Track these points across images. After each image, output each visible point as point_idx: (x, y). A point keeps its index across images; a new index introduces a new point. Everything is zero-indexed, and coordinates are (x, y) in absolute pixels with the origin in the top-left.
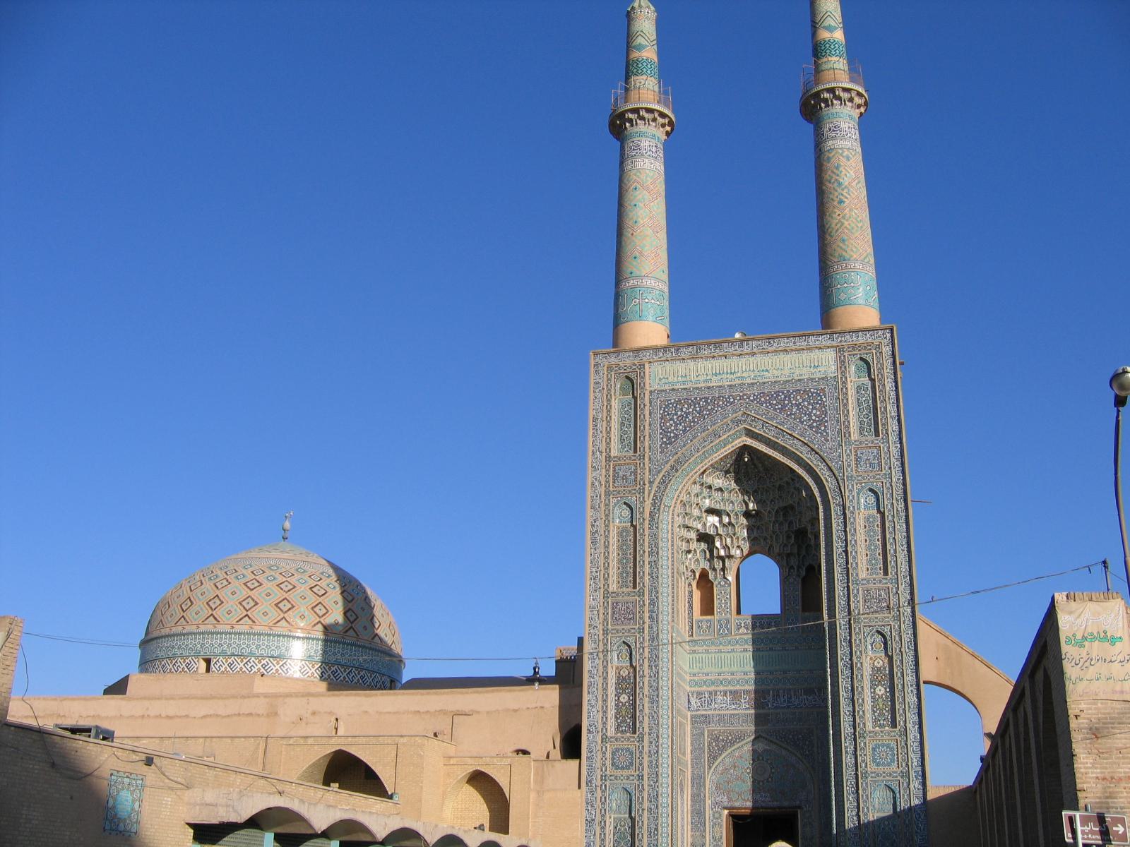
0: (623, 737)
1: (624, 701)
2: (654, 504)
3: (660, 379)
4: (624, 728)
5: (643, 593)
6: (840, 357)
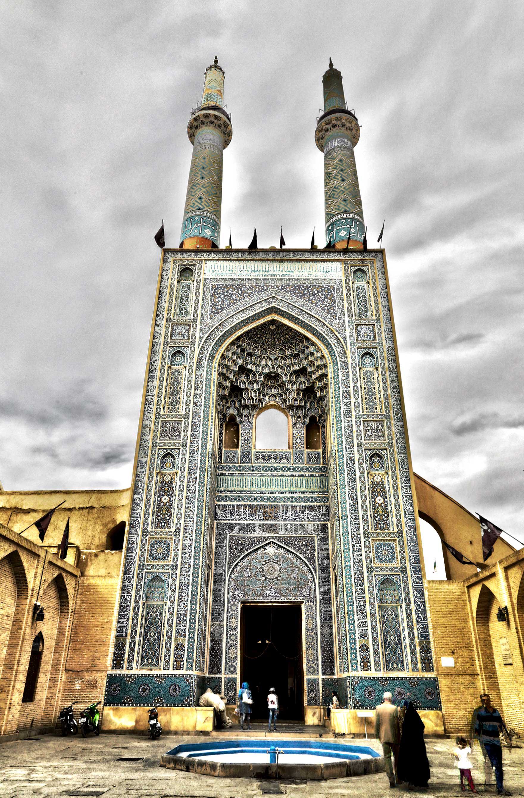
0: (161, 532)
1: (165, 501)
2: (201, 353)
3: (213, 271)
4: (163, 524)
5: (189, 416)
6: (345, 267)
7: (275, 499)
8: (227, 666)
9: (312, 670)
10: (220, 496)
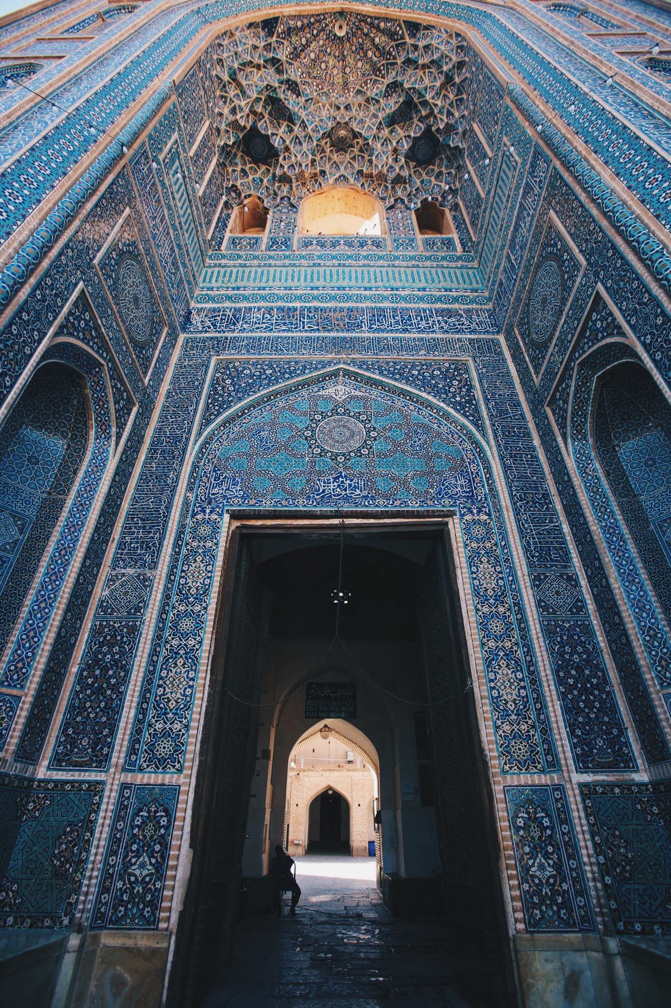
7: (349, 298)
8: (146, 736)
9: (521, 749)
10: (207, 295)
